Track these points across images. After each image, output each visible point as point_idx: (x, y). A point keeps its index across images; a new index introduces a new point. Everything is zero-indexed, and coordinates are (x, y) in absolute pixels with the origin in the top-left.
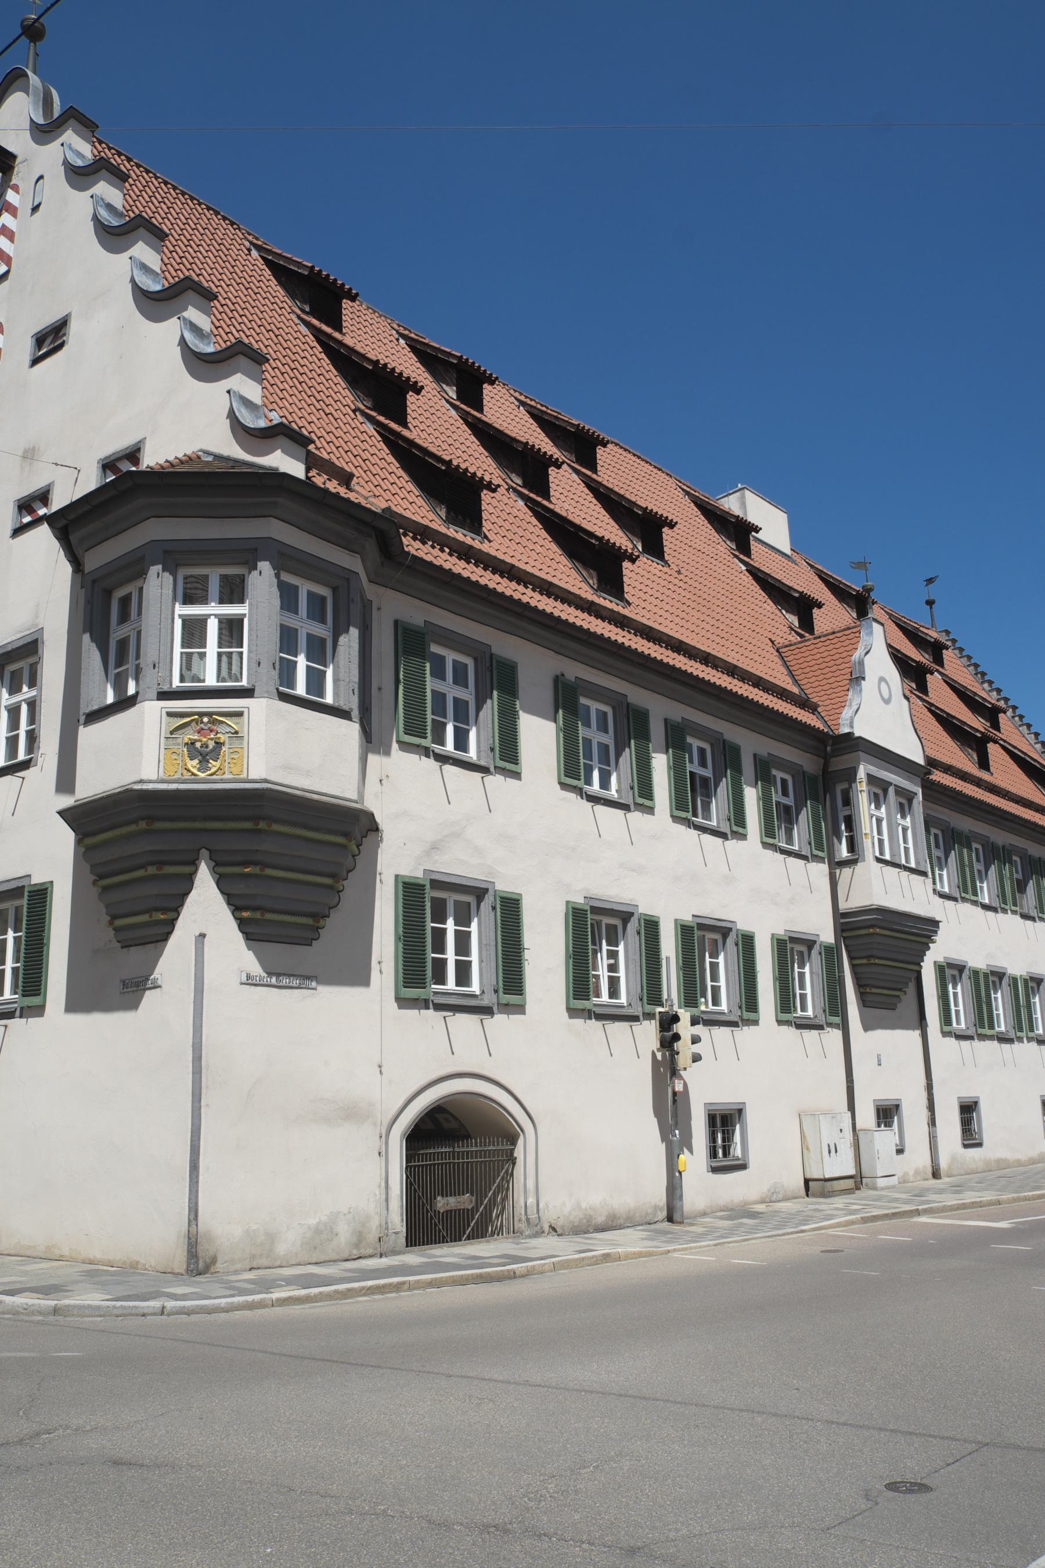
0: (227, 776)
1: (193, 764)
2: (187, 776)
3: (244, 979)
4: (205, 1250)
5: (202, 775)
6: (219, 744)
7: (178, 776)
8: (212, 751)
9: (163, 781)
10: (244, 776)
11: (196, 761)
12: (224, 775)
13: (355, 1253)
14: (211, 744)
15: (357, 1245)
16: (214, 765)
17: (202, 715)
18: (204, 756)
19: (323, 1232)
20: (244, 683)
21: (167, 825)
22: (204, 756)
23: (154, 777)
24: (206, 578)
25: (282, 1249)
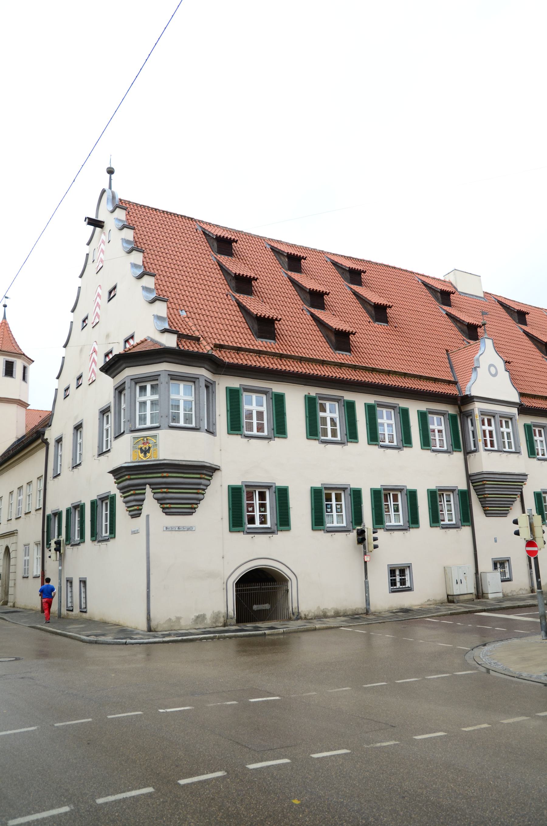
0: (153, 459)
1: (142, 455)
3: (165, 529)
4: (153, 624)
5: (145, 459)
6: (149, 448)
7: (137, 460)
10: (158, 458)
11: (143, 454)
13: (214, 625)
15: (215, 623)
18: (145, 452)
19: (200, 618)
22: (145, 452)
23: (130, 461)
24: (146, 386)
25: (183, 623)
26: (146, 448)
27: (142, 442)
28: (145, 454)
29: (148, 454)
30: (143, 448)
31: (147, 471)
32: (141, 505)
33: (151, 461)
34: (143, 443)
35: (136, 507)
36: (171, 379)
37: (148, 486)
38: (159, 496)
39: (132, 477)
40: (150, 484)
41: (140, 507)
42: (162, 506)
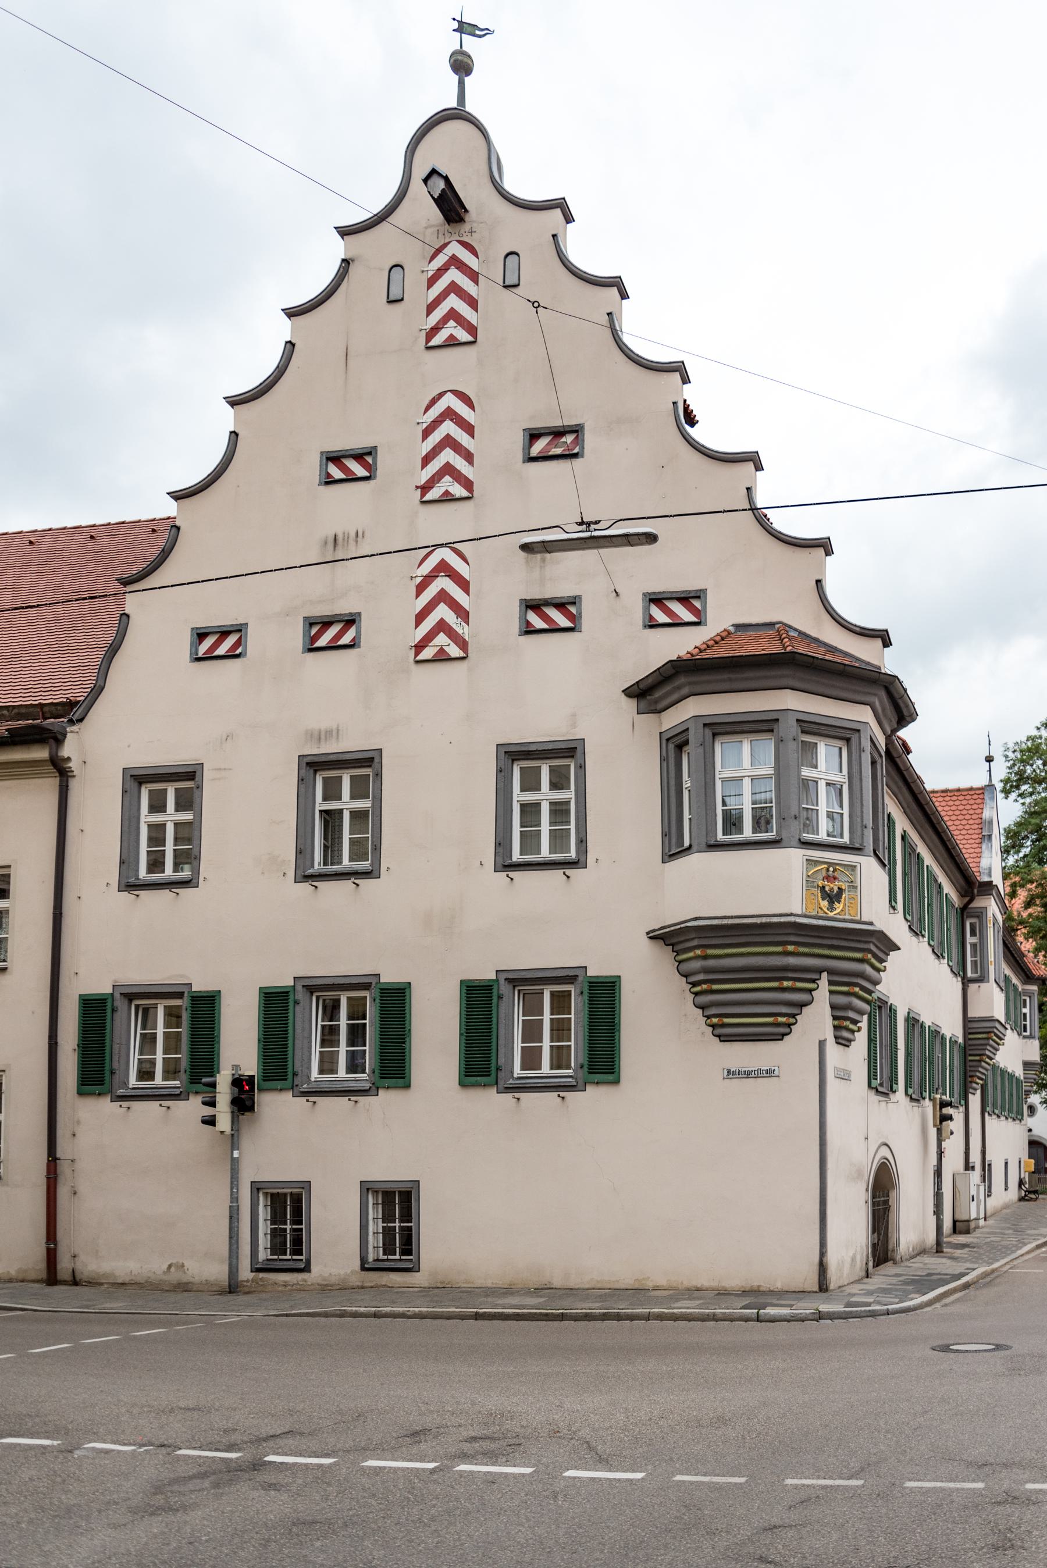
0: (847, 917)
1: (825, 904)
2: (821, 914)
5: (831, 914)
7: (814, 913)
8: (836, 895)
9: (805, 916)
10: (858, 918)
12: (840, 914)
14: (836, 889)
16: (839, 907)
17: (830, 864)
18: (833, 898)
20: (846, 839)
21: (806, 950)
22: (833, 898)
26: (832, 890)
27: (824, 873)
28: (831, 902)
29: (836, 905)
30: (827, 889)
31: (835, 942)
32: (794, 1016)
33: (844, 921)
34: (827, 878)
35: (781, 1019)
36: (803, 732)
37: (825, 975)
38: (842, 1000)
39: (801, 949)
40: (831, 972)
41: (792, 1020)
42: (836, 1023)
